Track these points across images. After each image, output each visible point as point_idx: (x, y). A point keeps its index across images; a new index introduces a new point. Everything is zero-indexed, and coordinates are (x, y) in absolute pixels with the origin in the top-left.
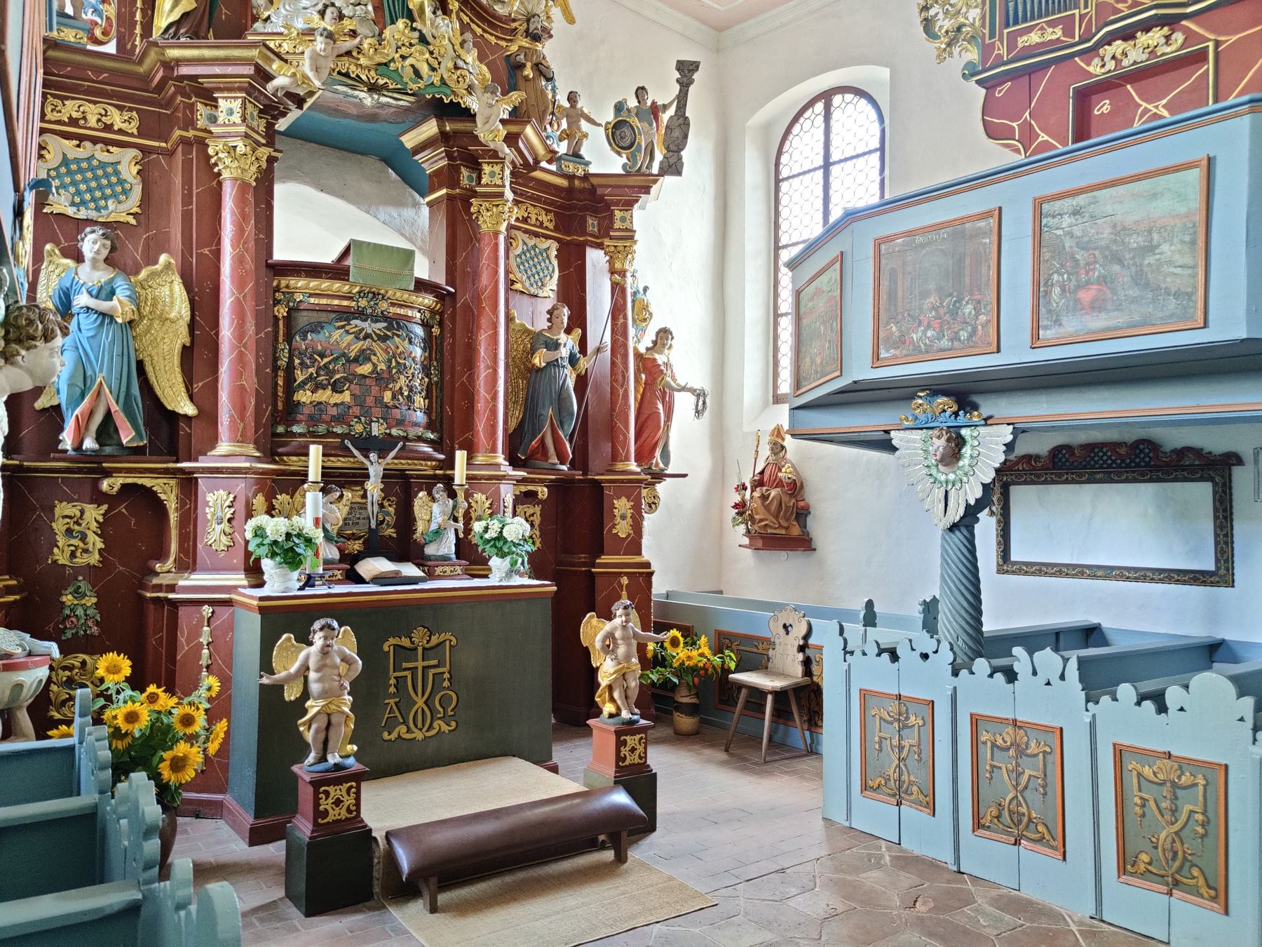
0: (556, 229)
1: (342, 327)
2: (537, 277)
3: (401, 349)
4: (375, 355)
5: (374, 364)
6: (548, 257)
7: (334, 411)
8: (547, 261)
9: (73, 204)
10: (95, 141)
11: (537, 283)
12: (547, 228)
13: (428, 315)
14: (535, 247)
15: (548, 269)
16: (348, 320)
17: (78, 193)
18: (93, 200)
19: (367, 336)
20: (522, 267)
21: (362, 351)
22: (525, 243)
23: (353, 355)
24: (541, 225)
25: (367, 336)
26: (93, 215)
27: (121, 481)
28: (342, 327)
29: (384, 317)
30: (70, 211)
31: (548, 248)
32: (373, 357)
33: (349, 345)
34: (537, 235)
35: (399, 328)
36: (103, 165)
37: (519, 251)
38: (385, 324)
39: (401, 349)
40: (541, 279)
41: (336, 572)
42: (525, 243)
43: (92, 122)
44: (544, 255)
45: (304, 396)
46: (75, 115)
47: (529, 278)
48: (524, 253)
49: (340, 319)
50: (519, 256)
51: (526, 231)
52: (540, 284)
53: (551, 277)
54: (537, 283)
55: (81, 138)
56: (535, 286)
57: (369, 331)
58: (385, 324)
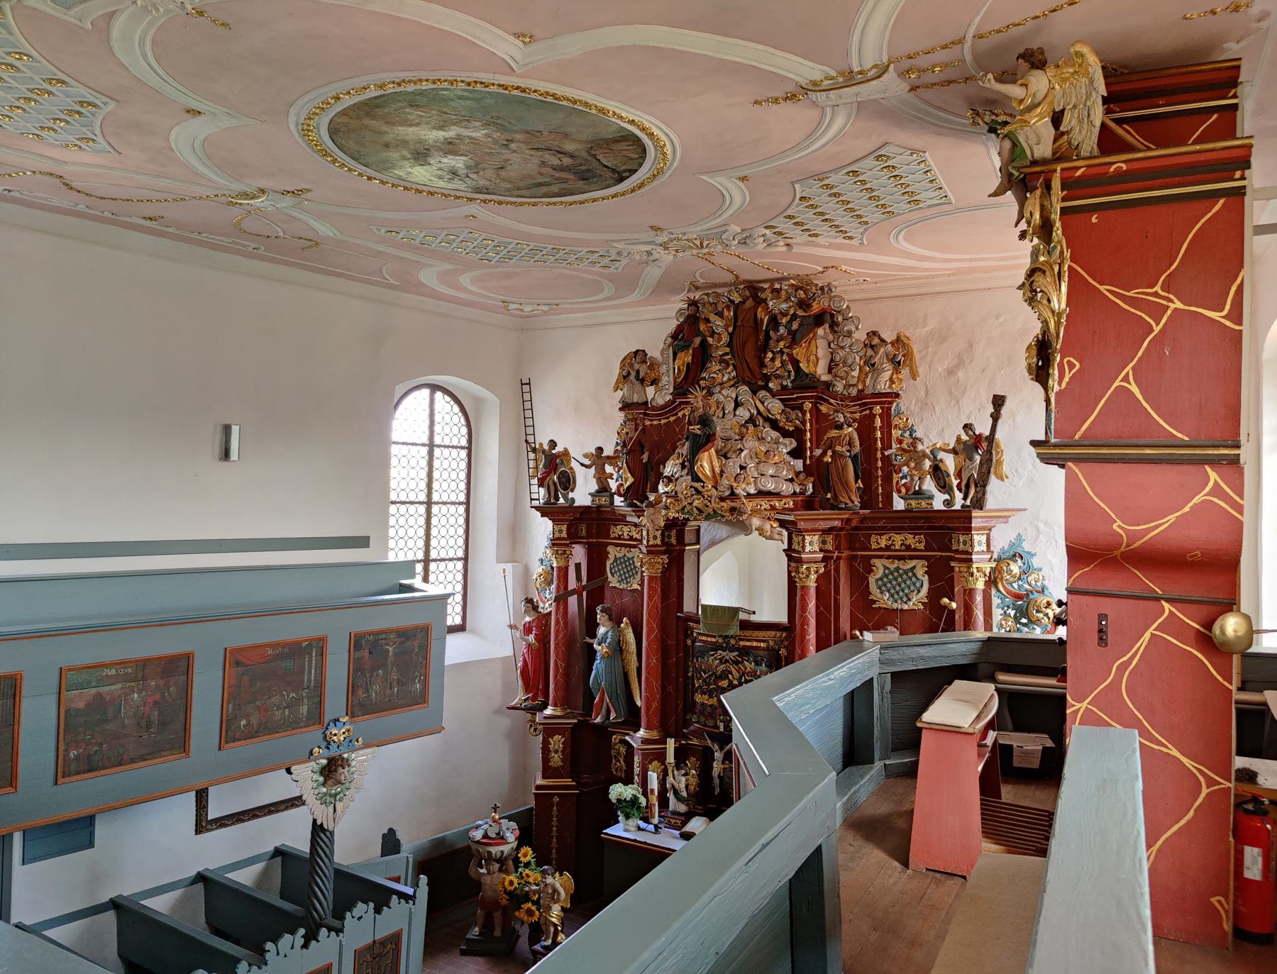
0: (927, 549)
1: (713, 655)
2: (901, 594)
3: (748, 669)
4: (731, 674)
5: (729, 680)
6: (914, 575)
7: (709, 710)
8: (914, 579)
9: (619, 582)
10: (626, 546)
11: (901, 599)
12: (915, 550)
13: (771, 643)
14: (897, 569)
15: (914, 584)
16: (716, 650)
17: (621, 575)
18: (626, 578)
19: (727, 661)
20: (884, 588)
21: (723, 671)
22: (886, 568)
23: (718, 673)
24: (908, 548)
25: (727, 661)
26: (625, 586)
27: (619, 737)
28: (713, 655)
29: (738, 649)
30: (617, 585)
31: (914, 567)
32: (730, 676)
33: (717, 667)
34: (900, 558)
35: (747, 654)
36: (629, 559)
37: (879, 576)
38: (737, 653)
39: (748, 669)
40: (907, 595)
41: (678, 821)
42: (886, 568)
43: (625, 534)
44: (910, 574)
45: (699, 698)
46: (620, 533)
47: (892, 596)
48: (886, 576)
49: (712, 650)
50: (881, 579)
51: (888, 557)
52: (905, 599)
53: (919, 592)
54: (901, 599)
55: (621, 545)
56: (899, 601)
57: (728, 658)
58: (737, 653)
